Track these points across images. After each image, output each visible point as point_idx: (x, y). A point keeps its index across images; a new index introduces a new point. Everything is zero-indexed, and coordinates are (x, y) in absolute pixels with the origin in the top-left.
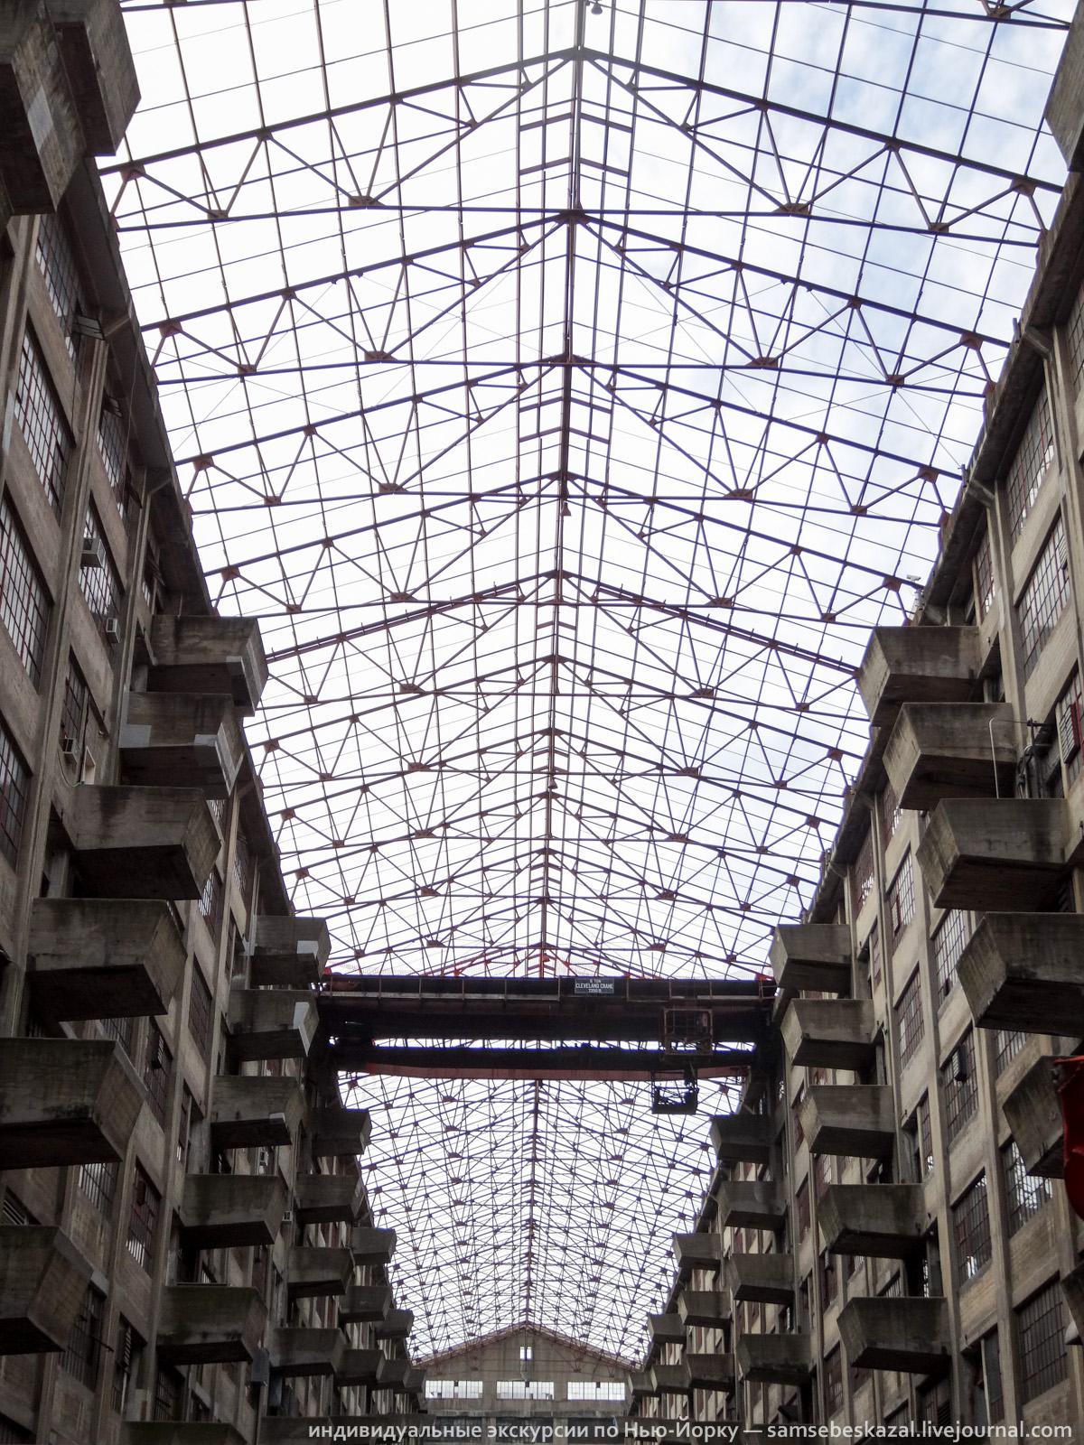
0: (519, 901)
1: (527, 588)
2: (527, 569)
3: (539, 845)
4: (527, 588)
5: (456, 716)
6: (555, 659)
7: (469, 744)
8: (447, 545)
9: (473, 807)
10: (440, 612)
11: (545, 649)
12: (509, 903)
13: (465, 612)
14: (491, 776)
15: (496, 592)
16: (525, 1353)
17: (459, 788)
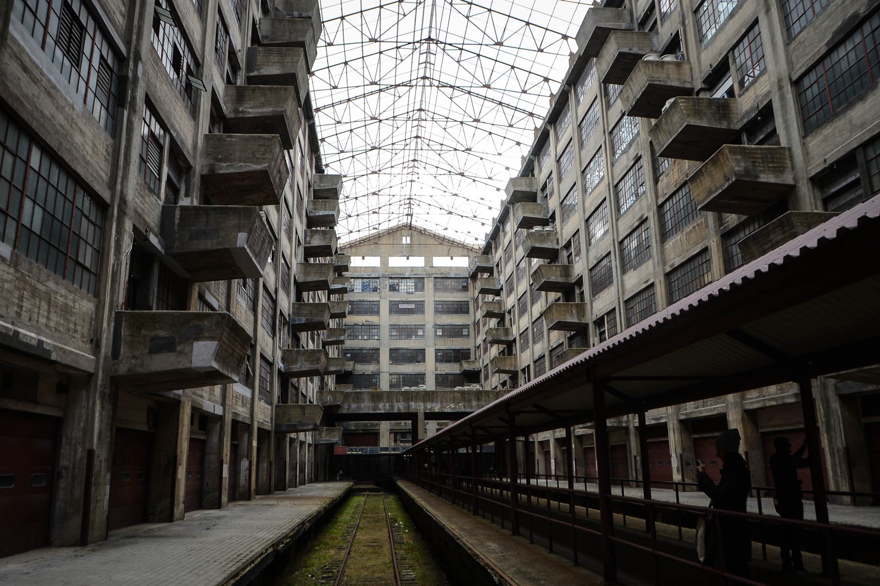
0: (400, 215)
1: (414, 83)
2: (414, 77)
3: (408, 197)
4: (414, 83)
5: (386, 129)
6: (417, 137)
7: (389, 141)
8: (388, 62)
9: (389, 165)
10: (384, 91)
11: (421, 75)
12: (397, 216)
13: (392, 91)
14: (397, 151)
15: (403, 85)
16: (406, 240)
17: (385, 156)
